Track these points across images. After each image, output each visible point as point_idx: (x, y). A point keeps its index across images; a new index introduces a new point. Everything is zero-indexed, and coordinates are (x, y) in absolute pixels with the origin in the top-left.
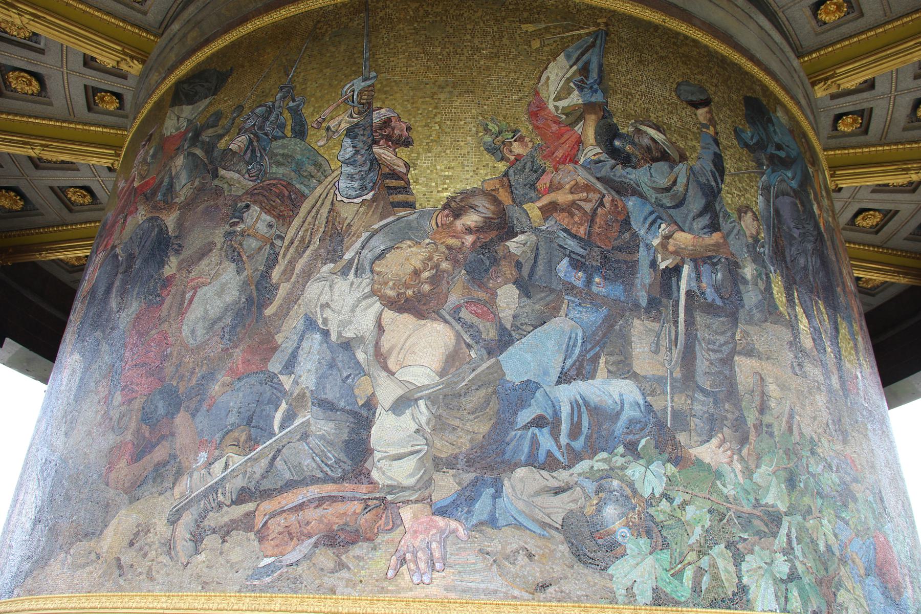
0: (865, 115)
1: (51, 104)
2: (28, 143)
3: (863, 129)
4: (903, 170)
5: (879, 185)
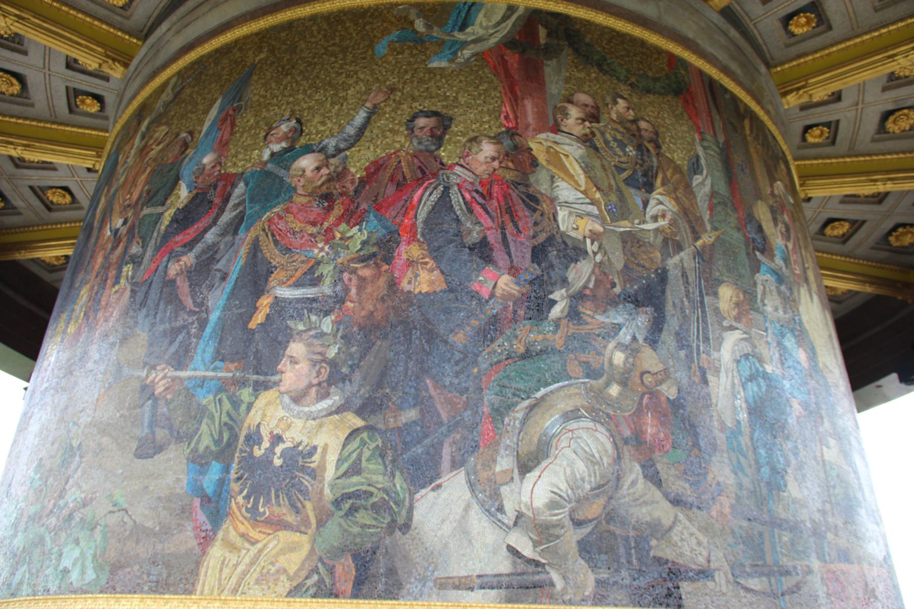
0: (833, 126)
1: (32, 105)
2: (11, 143)
3: (829, 141)
4: (872, 181)
5: (846, 196)
